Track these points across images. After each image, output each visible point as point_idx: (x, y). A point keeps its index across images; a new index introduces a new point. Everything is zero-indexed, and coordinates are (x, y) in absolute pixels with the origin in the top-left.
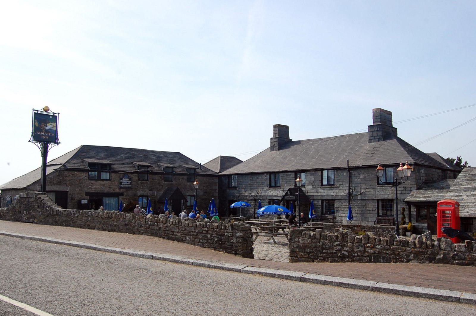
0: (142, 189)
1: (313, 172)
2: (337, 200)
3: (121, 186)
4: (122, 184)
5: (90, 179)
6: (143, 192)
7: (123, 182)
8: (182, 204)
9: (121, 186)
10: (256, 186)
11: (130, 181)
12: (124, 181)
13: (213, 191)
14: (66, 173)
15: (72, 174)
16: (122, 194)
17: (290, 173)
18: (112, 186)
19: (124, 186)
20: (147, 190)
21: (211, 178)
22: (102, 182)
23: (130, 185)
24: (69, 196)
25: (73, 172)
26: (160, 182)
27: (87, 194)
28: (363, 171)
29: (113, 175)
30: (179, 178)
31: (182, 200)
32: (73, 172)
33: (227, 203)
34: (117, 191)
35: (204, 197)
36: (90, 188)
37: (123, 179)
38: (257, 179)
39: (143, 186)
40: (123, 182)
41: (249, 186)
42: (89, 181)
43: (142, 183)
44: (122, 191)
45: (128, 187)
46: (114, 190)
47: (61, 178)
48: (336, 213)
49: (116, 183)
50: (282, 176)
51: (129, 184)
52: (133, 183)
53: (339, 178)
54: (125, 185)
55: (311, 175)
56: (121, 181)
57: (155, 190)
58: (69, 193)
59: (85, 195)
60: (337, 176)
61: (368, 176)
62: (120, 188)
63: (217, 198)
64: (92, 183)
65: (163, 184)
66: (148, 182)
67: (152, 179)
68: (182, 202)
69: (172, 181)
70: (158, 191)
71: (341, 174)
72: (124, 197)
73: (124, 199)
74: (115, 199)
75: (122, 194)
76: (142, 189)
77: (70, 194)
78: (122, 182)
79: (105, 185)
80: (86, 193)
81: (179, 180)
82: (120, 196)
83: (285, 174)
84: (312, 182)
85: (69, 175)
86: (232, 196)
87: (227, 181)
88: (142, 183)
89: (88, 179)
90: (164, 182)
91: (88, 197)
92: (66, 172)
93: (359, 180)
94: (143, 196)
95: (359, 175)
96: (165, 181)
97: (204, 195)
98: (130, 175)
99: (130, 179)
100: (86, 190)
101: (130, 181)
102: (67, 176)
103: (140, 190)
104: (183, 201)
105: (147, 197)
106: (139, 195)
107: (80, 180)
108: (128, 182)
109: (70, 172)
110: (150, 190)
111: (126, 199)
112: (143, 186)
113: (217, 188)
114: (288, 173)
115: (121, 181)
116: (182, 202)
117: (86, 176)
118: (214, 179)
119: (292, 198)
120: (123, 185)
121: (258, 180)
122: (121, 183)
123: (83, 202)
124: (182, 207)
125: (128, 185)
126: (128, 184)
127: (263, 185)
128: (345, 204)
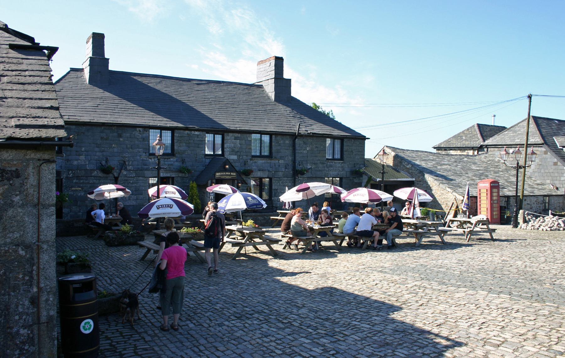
1: (239, 135)
2: (275, 179)
10: (116, 150)
17: (196, 133)
28: (310, 140)
38: (120, 136)
41: (97, 149)
48: (275, 196)
50: (178, 137)
53: (279, 147)
55: (236, 138)
60: (277, 144)
61: (316, 147)
71: (282, 142)
83: (187, 132)
84: (236, 150)
93: (305, 152)
95: (304, 146)
114: (193, 132)
119: (230, 175)
121: (121, 139)
127: (135, 150)
128: (286, 184)
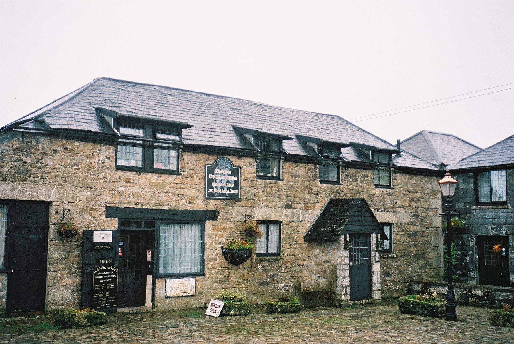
0: (267, 201)
3: (211, 191)
4: (214, 184)
5: (119, 168)
6: (269, 210)
7: (216, 180)
8: (374, 247)
9: (211, 191)
11: (236, 178)
12: (218, 177)
13: (430, 213)
14: (45, 143)
15: (66, 149)
16: (213, 215)
18: (183, 192)
19: (219, 191)
20: (279, 205)
21: (426, 179)
22: (154, 178)
23: (234, 188)
24: (54, 219)
25: (69, 142)
26: (312, 182)
27: (111, 212)
29: (189, 158)
30: (355, 176)
31: (374, 236)
32: (67, 144)
33: (473, 244)
34: (200, 205)
35: (412, 228)
36: (122, 194)
37: (217, 171)
39: (268, 193)
40: (216, 180)
42: (119, 173)
43: (266, 186)
44: (212, 205)
45: (230, 195)
46: (190, 203)
47: (27, 160)
49: (197, 181)
51: (232, 186)
52: (243, 184)
54: (222, 188)
56: (211, 176)
57: (299, 206)
58: (53, 209)
59: (104, 216)
62: (209, 196)
63: (440, 230)
64: (128, 181)
65: (317, 190)
66: (280, 182)
67: (292, 176)
68: (374, 241)
69: (337, 183)
70: (307, 208)
72: (218, 223)
73: (217, 229)
74: (196, 230)
75: (213, 215)
76: (267, 201)
77: (57, 212)
78: (212, 180)
79: (165, 187)
80: (108, 208)
81: (356, 180)
82: (206, 221)
85: (56, 151)
86: (490, 227)
87: (472, 185)
88: (266, 186)
89: (114, 165)
90: (320, 185)
91: (114, 223)
92: (43, 140)
94: (267, 223)
96: (322, 182)
97: (412, 223)
98: (236, 161)
99: (236, 172)
100: (109, 199)
101: (236, 178)
102: (45, 155)
103: (262, 205)
104: (377, 238)
105: (278, 223)
106: (258, 217)
107: (90, 167)
108: (228, 182)
109: (59, 142)
110: (288, 206)
111: (225, 230)
112: (268, 193)
113: (440, 206)
115: (211, 176)
116: (374, 241)
117: (108, 158)
118: (431, 182)
120: (216, 187)
122: (209, 183)
123: (98, 237)
124: (373, 254)
125: (229, 188)
126: (229, 185)
